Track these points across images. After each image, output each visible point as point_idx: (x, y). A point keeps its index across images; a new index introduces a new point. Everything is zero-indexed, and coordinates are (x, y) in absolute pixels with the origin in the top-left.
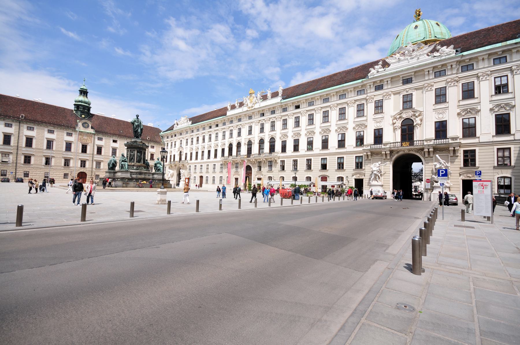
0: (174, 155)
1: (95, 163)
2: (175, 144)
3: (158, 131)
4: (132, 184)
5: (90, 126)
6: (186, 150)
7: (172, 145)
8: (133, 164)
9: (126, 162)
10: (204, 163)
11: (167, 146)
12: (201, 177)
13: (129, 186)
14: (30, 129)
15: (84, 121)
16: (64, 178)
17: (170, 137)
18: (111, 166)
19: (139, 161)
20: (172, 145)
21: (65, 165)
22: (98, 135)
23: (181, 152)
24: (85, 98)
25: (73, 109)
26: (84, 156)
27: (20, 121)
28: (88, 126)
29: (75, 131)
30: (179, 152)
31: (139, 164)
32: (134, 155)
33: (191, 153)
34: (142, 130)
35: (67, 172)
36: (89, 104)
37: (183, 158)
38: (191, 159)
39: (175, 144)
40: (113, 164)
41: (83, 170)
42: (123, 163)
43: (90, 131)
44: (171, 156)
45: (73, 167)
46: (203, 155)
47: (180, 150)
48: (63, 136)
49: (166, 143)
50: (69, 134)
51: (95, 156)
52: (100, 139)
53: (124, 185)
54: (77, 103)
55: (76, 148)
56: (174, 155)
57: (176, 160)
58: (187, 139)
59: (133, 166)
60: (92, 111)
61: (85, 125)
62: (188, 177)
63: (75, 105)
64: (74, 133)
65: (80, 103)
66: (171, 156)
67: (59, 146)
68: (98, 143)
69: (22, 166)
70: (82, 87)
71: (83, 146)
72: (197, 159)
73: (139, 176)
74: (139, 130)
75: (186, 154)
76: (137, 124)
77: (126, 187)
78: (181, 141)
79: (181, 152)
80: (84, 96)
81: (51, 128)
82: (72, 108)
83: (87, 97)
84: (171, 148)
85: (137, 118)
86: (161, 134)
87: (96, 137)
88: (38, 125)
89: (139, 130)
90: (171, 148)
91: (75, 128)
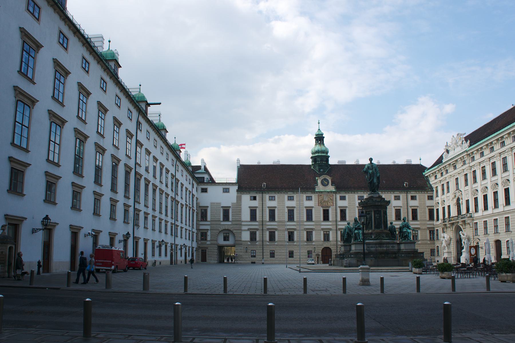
0: (449, 206)
1: (339, 233)
2: (448, 188)
3: (420, 168)
6: (467, 195)
7: (443, 190)
8: (370, 231)
9: (360, 229)
10: (499, 214)
11: (437, 191)
12: (498, 243)
14: (272, 199)
15: (322, 177)
16: (309, 257)
17: (439, 175)
18: (346, 237)
19: (377, 226)
20: (443, 190)
21: (308, 240)
23: (458, 199)
24: (322, 146)
25: (311, 164)
26: (326, 225)
27: (262, 191)
28: (328, 184)
30: (455, 200)
32: (372, 217)
33: (476, 199)
34: (378, 178)
35: (310, 249)
36: (327, 153)
37: (464, 211)
38: (476, 211)
39: (448, 188)
40: (348, 233)
41: (327, 244)
42: (356, 231)
44: (444, 208)
45: (316, 241)
46: (496, 201)
47: (457, 195)
49: (434, 186)
50: (309, 198)
52: (343, 198)
54: (314, 155)
55: (318, 214)
56: (449, 206)
57: (452, 215)
58: (466, 175)
59: (371, 234)
61: (324, 183)
62: (475, 244)
63: (312, 158)
65: (317, 155)
66: (444, 208)
67: (300, 215)
68: (341, 203)
69: (268, 243)
71: (324, 210)
72: (486, 208)
74: (375, 180)
75: (467, 201)
76: (371, 171)
78: (457, 179)
79: (458, 199)
80: (320, 144)
81: (291, 194)
82: (309, 162)
83: (323, 144)
84: (443, 194)
85: (371, 162)
86: (426, 173)
87: (338, 196)
89: (375, 180)
90: (443, 194)
91: (314, 189)
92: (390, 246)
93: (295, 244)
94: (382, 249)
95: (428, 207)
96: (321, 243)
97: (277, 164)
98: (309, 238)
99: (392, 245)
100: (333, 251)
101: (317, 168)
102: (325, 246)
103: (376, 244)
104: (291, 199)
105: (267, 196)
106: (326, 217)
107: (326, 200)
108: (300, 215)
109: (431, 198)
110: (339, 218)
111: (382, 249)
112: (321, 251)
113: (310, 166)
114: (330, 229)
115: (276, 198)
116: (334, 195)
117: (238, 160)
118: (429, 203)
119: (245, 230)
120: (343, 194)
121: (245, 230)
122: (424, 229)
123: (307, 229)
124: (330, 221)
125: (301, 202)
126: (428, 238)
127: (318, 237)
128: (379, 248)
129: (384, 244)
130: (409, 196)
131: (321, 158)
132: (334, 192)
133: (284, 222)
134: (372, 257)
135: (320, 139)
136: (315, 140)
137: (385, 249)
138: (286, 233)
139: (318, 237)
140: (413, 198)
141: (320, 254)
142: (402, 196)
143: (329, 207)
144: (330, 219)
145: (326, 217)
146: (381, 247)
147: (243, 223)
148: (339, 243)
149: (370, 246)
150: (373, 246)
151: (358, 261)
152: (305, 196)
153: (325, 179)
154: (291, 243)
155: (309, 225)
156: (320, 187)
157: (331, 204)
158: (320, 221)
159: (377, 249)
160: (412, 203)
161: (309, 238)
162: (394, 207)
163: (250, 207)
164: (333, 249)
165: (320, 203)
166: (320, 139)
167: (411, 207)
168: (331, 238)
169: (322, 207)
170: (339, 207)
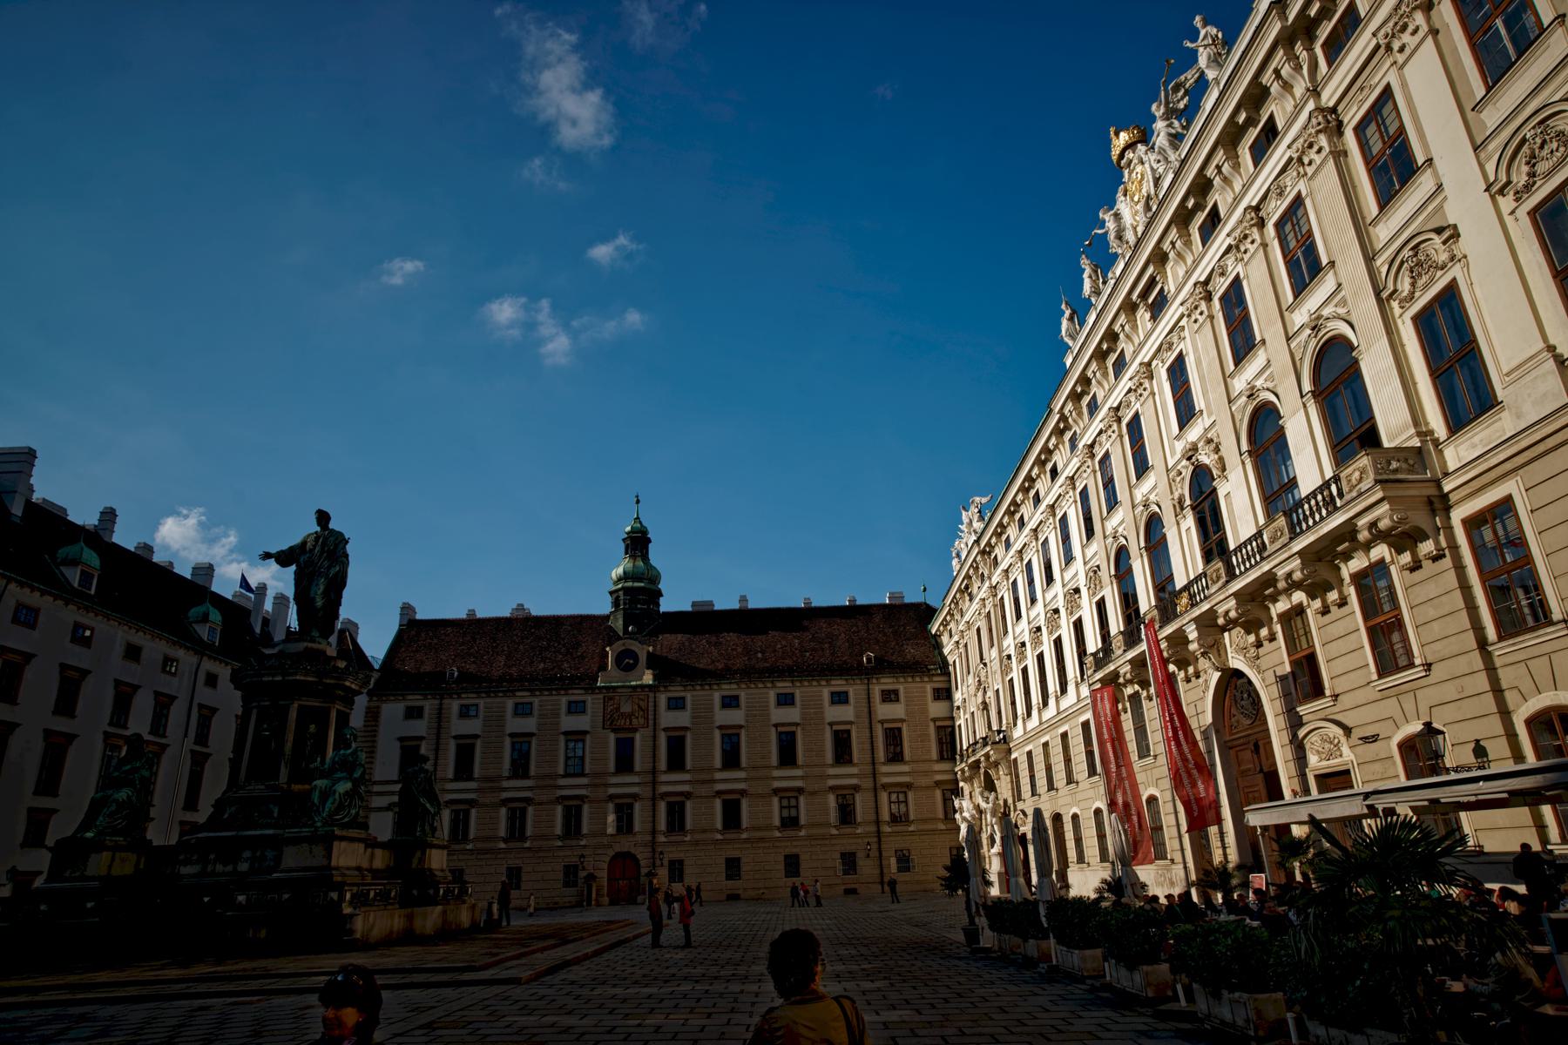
1: (662, 807)
15: (619, 646)
29: (592, 689)
30: (980, 694)
41: (625, 844)
48: (557, 715)
50: (576, 708)
51: (664, 778)
60: (667, 605)
63: (611, 593)
64: (589, 698)
68: (669, 719)
71: (618, 741)
82: (603, 606)
87: (663, 699)
93: (527, 845)
95: (934, 720)
96: (605, 841)
97: (520, 614)
100: (642, 863)
101: (621, 622)
102: (618, 848)
105: (454, 706)
106: (625, 762)
107: (626, 708)
109: (945, 694)
110: (663, 764)
114: (635, 797)
117: (407, 609)
118: (937, 709)
119: (380, 809)
120: (676, 691)
121: (380, 809)
122: (928, 787)
124: (638, 774)
126: (941, 815)
130: (876, 691)
131: (639, 594)
133: (500, 778)
135: (638, 543)
136: (622, 546)
140: (890, 696)
142: (854, 690)
143: (635, 730)
144: (637, 767)
145: (625, 762)
147: (376, 788)
148: (662, 839)
152: (564, 700)
156: (610, 676)
157: (642, 721)
160: (884, 711)
163: (401, 739)
164: (643, 855)
165: (611, 721)
166: (638, 543)
167: (882, 722)
169: (614, 731)
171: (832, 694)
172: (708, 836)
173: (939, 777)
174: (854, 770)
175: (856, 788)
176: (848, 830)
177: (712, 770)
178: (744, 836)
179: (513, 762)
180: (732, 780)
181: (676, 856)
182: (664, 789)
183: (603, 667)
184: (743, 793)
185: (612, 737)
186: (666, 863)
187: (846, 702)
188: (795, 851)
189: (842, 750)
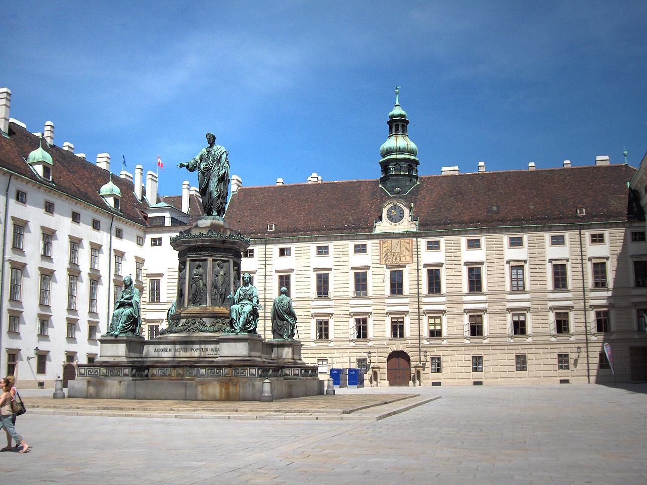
4: (114, 385)
5: (407, 212)
13: (106, 391)
22: (426, 235)
31: (194, 309)
41: (398, 345)
43: (407, 224)
52: (433, 246)
53: (92, 389)
55: (379, 282)
60: (422, 172)
67: (342, 285)
68: (430, 257)
70: (390, 114)
73: (183, 354)
77: (98, 396)
88: (298, 241)
91: (372, 228)
92: (210, 347)
93: (332, 344)
94: (188, 354)
95: (632, 256)
98: (362, 331)
99: (213, 346)
103: (174, 343)
104: (323, 251)
105: (274, 249)
106: (397, 287)
108: (342, 285)
110: (424, 289)
111: (188, 354)
112: (385, 360)
113: (376, 183)
115: (293, 251)
116: (414, 239)
123: (355, 314)
125: (342, 257)
126: (635, 327)
127: (378, 329)
128: (183, 354)
129: (193, 343)
132: (413, 233)
134: (126, 375)
137: (196, 354)
138: (352, 322)
139: (378, 329)
141: (385, 365)
143: (404, 266)
145: (397, 287)
146: (186, 350)
148: (425, 342)
149: (162, 347)
150: (169, 347)
151: (89, 382)
153: (395, 207)
154: (322, 344)
155: (361, 305)
157: (408, 258)
158: (382, 297)
159: (177, 354)
160: (595, 251)
161: (362, 331)
162: (550, 261)
164: (413, 354)
165: (385, 258)
167: (590, 259)
168: (407, 332)
169: (388, 267)
170: (426, 265)
171: (552, 237)
172: (458, 341)
173: (635, 300)
174: (569, 295)
175: (570, 308)
176: (563, 338)
177: (461, 294)
178: (486, 341)
179: (319, 288)
180: (476, 302)
181: (436, 353)
182: (425, 308)
183: (381, 218)
184: (484, 311)
185: (387, 272)
186: (429, 359)
187: (563, 243)
188: (522, 352)
189: (560, 280)
